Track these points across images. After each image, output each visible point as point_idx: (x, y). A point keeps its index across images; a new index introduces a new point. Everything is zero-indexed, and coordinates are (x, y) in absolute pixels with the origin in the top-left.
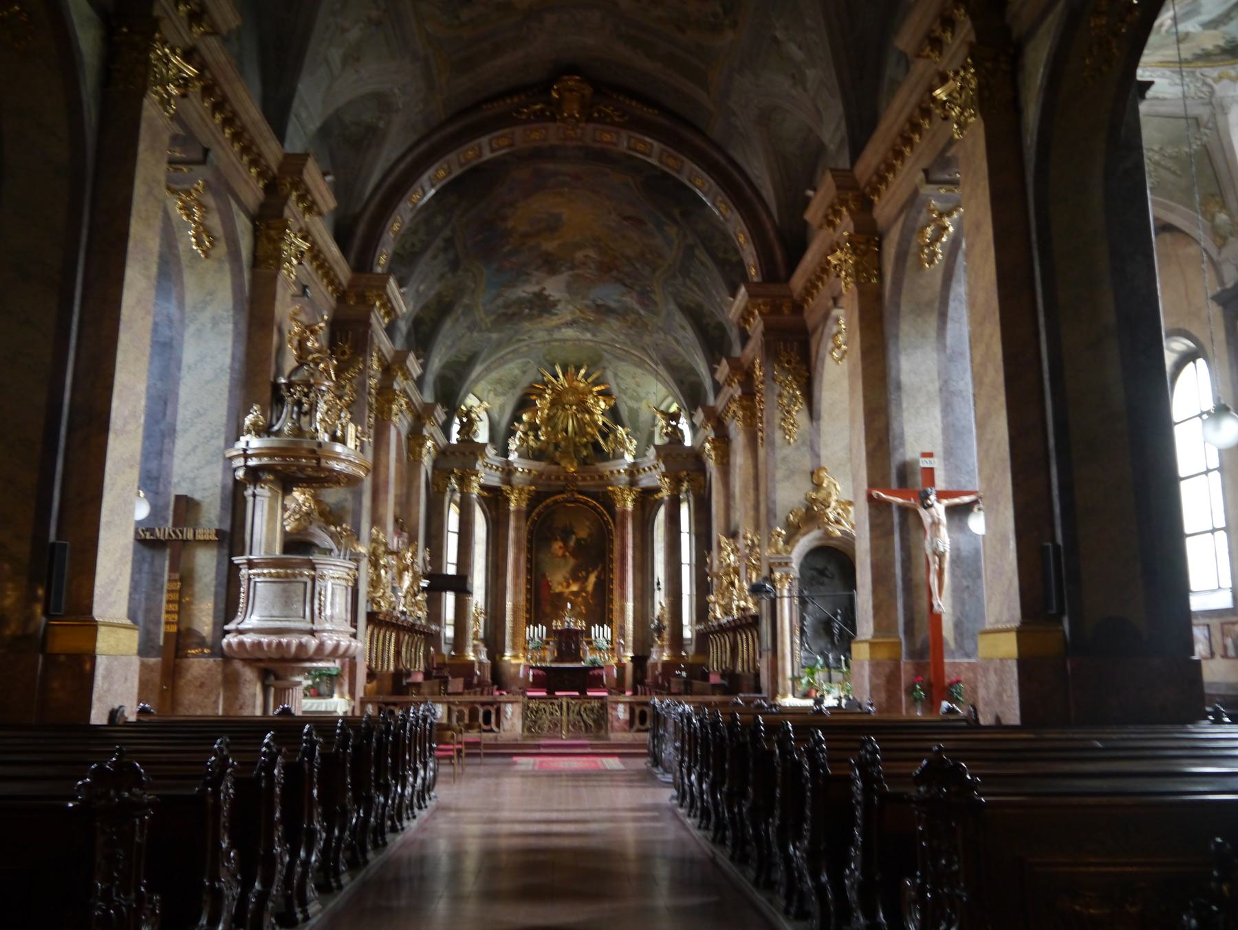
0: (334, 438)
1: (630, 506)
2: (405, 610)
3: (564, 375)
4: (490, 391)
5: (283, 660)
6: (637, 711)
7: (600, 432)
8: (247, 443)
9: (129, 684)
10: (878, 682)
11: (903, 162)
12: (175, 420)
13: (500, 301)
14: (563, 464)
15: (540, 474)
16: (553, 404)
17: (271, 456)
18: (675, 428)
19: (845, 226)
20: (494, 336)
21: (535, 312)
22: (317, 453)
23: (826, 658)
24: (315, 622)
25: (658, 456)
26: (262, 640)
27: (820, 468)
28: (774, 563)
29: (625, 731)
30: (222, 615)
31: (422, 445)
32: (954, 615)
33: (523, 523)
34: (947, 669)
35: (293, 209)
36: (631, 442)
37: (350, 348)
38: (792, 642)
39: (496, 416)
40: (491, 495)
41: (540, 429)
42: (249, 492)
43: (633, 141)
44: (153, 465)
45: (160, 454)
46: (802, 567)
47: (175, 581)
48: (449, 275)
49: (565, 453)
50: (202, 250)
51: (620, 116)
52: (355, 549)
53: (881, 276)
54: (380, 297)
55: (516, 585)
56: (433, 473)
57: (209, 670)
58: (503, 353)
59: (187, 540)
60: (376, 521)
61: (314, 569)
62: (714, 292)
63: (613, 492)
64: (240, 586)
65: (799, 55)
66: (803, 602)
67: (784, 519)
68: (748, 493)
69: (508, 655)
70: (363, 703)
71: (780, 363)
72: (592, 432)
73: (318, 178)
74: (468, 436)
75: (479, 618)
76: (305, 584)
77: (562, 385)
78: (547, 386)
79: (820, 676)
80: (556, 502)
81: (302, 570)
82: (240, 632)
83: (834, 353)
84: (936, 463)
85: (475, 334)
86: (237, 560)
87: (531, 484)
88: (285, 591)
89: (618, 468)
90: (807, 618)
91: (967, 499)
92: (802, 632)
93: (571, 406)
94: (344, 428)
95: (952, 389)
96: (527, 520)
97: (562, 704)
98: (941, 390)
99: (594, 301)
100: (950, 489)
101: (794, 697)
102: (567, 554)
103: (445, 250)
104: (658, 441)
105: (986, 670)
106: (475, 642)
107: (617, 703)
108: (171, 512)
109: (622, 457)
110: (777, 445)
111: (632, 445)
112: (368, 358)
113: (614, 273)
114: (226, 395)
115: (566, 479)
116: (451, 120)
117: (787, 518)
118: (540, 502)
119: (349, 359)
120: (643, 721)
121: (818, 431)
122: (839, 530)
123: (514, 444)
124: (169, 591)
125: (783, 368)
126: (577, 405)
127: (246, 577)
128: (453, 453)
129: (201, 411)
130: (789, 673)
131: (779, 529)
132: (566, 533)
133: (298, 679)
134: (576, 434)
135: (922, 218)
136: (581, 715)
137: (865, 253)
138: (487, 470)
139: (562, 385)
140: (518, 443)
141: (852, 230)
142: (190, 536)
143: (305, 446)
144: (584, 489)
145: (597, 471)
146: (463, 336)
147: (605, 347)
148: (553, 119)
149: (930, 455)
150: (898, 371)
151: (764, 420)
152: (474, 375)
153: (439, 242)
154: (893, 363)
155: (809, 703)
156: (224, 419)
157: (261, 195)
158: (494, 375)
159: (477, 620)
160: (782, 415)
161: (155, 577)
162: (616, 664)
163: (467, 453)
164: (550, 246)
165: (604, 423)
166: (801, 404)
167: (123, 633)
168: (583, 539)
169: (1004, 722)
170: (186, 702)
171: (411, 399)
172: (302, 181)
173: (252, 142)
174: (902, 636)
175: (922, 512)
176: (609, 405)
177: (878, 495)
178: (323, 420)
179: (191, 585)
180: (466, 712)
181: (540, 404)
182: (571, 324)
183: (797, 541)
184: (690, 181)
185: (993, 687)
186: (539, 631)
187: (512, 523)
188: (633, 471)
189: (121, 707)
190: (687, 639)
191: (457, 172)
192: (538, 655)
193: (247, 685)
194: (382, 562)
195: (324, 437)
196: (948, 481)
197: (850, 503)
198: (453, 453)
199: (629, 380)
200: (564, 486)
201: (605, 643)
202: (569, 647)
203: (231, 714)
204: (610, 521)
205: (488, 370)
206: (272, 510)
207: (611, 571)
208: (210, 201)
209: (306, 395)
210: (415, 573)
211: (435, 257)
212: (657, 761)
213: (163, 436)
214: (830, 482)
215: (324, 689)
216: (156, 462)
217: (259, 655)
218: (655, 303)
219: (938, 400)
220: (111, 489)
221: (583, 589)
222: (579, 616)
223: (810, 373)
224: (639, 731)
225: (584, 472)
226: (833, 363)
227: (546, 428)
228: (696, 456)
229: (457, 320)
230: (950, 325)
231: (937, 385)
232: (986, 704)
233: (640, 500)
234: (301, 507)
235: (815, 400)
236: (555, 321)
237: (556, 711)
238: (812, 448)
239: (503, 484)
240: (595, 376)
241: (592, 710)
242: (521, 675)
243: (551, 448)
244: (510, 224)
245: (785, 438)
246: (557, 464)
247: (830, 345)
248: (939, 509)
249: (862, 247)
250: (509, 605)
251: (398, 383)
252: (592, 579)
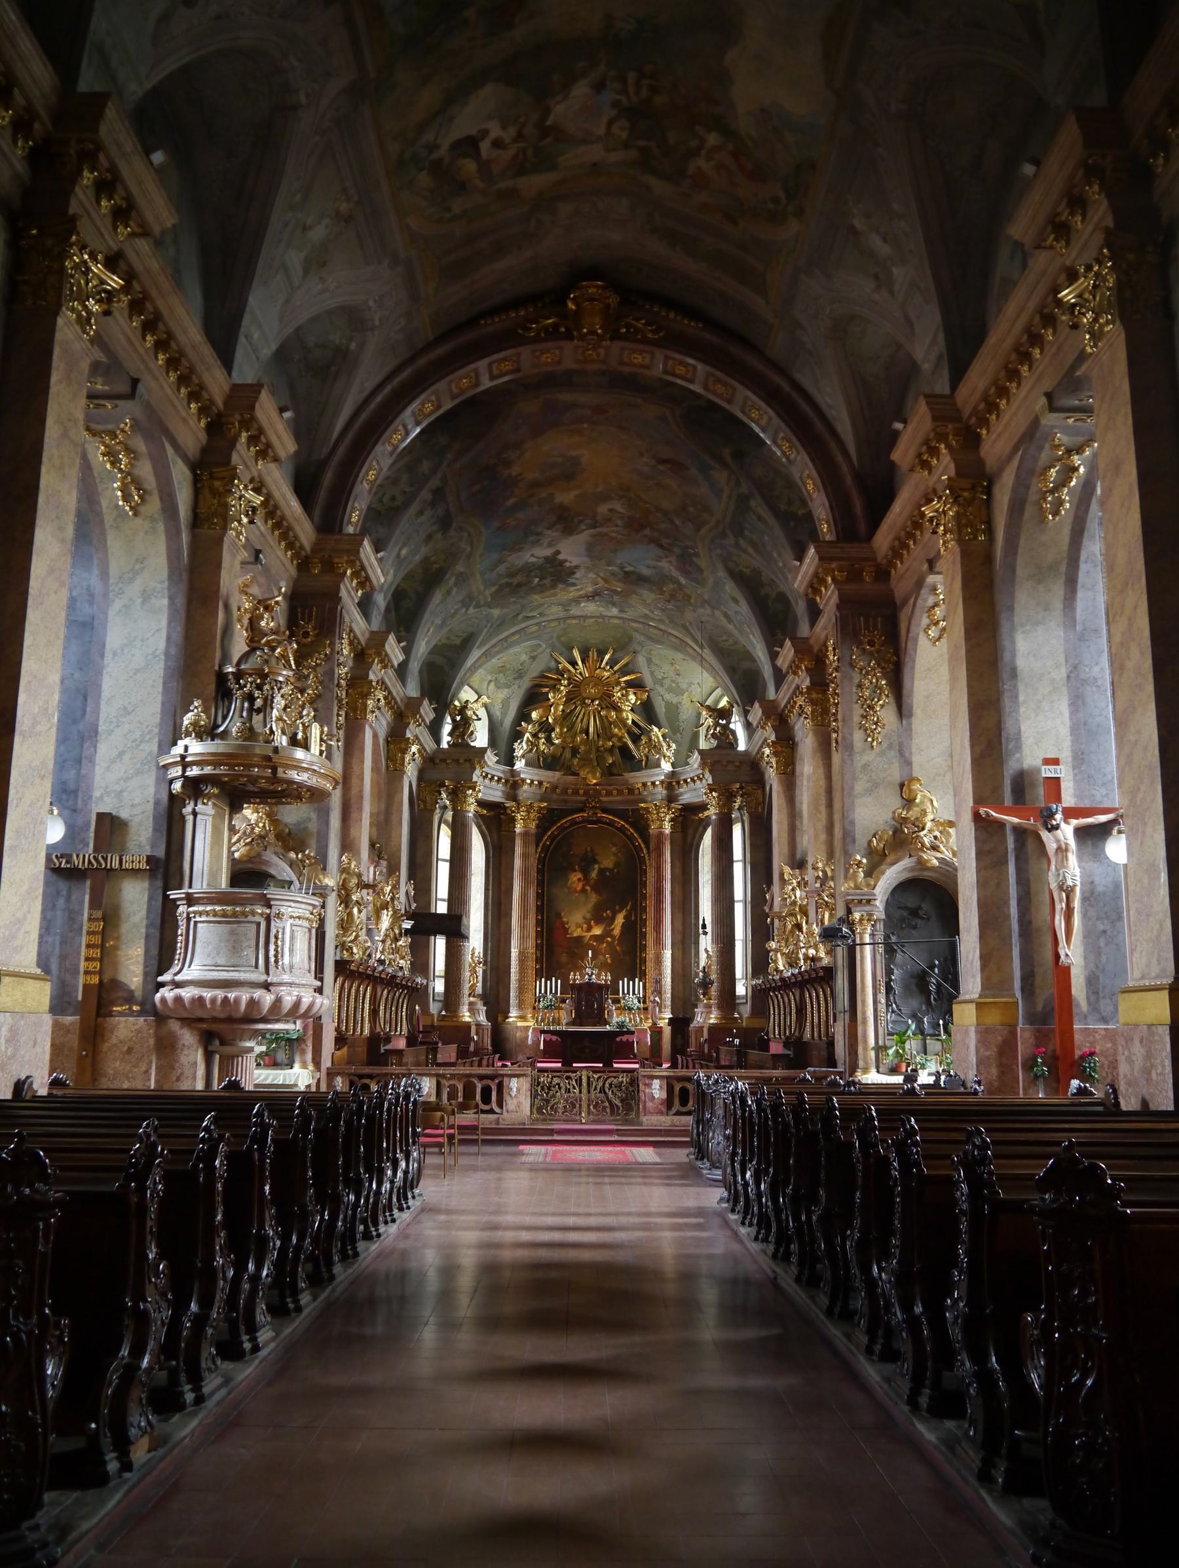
0: (294, 742)
1: (667, 828)
2: (383, 957)
3: (583, 661)
4: (490, 681)
5: (230, 1020)
6: (677, 1089)
7: (629, 732)
8: (186, 748)
9: (39, 1049)
10: (988, 1053)
11: (1019, 384)
12: (98, 719)
13: (502, 569)
14: (582, 774)
15: (554, 788)
16: (570, 698)
17: (216, 764)
18: (726, 727)
19: (944, 468)
20: (496, 612)
21: (547, 582)
22: (272, 761)
23: (919, 1022)
24: (271, 972)
25: (703, 764)
26: (205, 994)
27: (912, 779)
28: (853, 900)
29: (661, 1113)
30: (155, 963)
31: (404, 751)
32: (1086, 967)
33: (532, 849)
34: (1077, 1037)
35: (242, 455)
36: (669, 746)
37: (314, 628)
38: (875, 1002)
39: (498, 713)
40: (492, 813)
41: (553, 730)
42: (188, 809)
43: (670, 363)
44: (71, 774)
45: (79, 761)
46: (888, 905)
47: (97, 920)
48: (439, 536)
49: (586, 761)
50: (131, 507)
51: (655, 332)
52: (320, 881)
53: (990, 532)
54: (351, 563)
55: (523, 927)
56: (419, 785)
57: (139, 1031)
58: (506, 634)
59: (111, 869)
60: (347, 845)
61: (270, 907)
62: (775, 555)
63: (646, 809)
64: (177, 927)
65: (884, 250)
66: (890, 951)
67: (865, 845)
68: (820, 812)
69: (514, 1013)
70: (331, 1075)
71: (859, 644)
72: (620, 734)
73: (274, 414)
74: (463, 739)
75: (477, 969)
76: (259, 924)
77: (581, 674)
78: (563, 676)
79: (912, 1045)
80: (574, 823)
81: (254, 907)
82: (178, 985)
83: (930, 632)
84: (1063, 772)
85: (471, 610)
86: (173, 894)
87: (541, 801)
88: (232, 933)
89: (653, 780)
90: (895, 971)
91: (1103, 818)
92: (889, 989)
93: (592, 701)
94: (306, 728)
95: (1083, 676)
96: (537, 846)
97: (581, 1077)
98: (1068, 677)
99: (622, 568)
100: (1082, 805)
101: (878, 1072)
102: (588, 888)
103: (433, 504)
104: (703, 745)
105: (1129, 1040)
106: (472, 999)
107: (653, 1077)
108: (92, 835)
109: (659, 766)
110: (855, 749)
111: (669, 750)
112: (337, 641)
113: (647, 532)
114: (160, 688)
115: (585, 793)
116: (441, 339)
117: (870, 842)
118: (554, 823)
119: (312, 642)
120: (684, 1103)
121: (909, 730)
122: (936, 858)
123: (520, 749)
124: (89, 933)
125: (864, 650)
126: (600, 699)
127: (185, 915)
128: (444, 760)
129: (130, 708)
130: (871, 1042)
131: (858, 857)
132: (586, 863)
133: (249, 1044)
134: (598, 736)
135: (1044, 456)
136: (605, 1093)
137: (969, 502)
138: (487, 781)
139: (581, 674)
140: (525, 747)
141: (953, 473)
142: (115, 864)
143: (258, 751)
144: (610, 806)
145: (626, 782)
146: (456, 613)
147: (635, 625)
148: (569, 336)
149: (1055, 762)
150: (1014, 656)
151: (839, 717)
152: (470, 662)
153: (425, 495)
154: (1006, 643)
155: (898, 1079)
156: (157, 719)
157: (203, 437)
158: (495, 662)
159: (473, 971)
160: (862, 712)
161: (72, 917)
162: (650, 1028)
163: (461, 761)
164: (565, 497)
165: (633, 721)
166: (887, 696)
167: (32, 985)
168: (607, 869)
169: (1153, 1107)
170: (111, 1072)
171: (390, 693)
172: (253, 418)
173: (192, 370)
174: (1018, 994)
175: (1045, 835)
176: (641, 699)
177: (987, 814)
178: (280, 719)
179: (116, 926)
180: (460, 1087)
181: (554, 697)
182: (593, 597)
183: (883, 873)
184: (743, 412)
185: (1139, 1061)
186: (556, 984)
187: (518, 850)
188: (672, 783)
189: (28, 1077)
190: (740, 997)
191: (448, 405)
192: (550, 1016)
193: (186, 1052)
194: (354, 898)
195: (282, 740)
196: (1078, 795)
197: (951, 824)
198: (444, 760)
199: (666, 668)
200: (584, 803)
201: (636, 1001)
202: (590, 1006)
203: (166, 1087)
204: (642, 845)
205: (487, 655)
206: (217, 831)
207: (644, 910)
208: (140, 445)
209: (259, 687)
210: (395, 912)
211: (421, 512)
212: (702, 1153)
213: (82, 739)
214: (924, 796)
215: (281, 1056)
216: (73, 772)
217: (200, 1014)
218: (701, 571)
219: (1065, 690)
220: (17, 806)
221: (608, 933)
222: (603, 967)
223: (898, 657)
224: (678, 1113)
225: (610, 785)
226: (929, 644)
227: (561, 730)
228: (752, 766)
229: (449, 592)
230: (1080, 594)
231: (1064, 671)
232: (1129, 1084)
233: (680, 819)
234: (253, 829)
235: (905, 692)
236: (573, 593)
237: (574, 1088)
238: (901, 753)
239: (507, 799)
240: (622, 662)
241: (619, 1086)
242: (530, 1042)
243: (568, 754)
244: (515, 470)
245: (866, 740)
247: (925, 621)
248: (1067, 831)
249: (966, 494)
251: (374, 673)
252: (620, 920)
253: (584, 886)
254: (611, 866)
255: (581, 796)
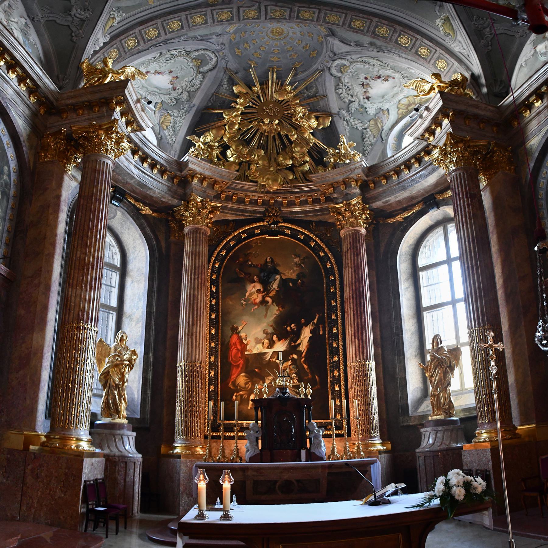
55: (191, 335)
80: (251, 234)
200: (264, 213)
221: (293, 349)
246: (256, 182)
250: (181, 365)
252: (306, 333)
253: (264, 297)
254: (294, 276)
255: (260, 206)
